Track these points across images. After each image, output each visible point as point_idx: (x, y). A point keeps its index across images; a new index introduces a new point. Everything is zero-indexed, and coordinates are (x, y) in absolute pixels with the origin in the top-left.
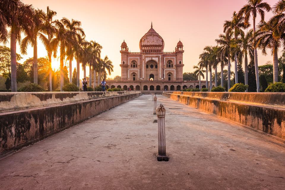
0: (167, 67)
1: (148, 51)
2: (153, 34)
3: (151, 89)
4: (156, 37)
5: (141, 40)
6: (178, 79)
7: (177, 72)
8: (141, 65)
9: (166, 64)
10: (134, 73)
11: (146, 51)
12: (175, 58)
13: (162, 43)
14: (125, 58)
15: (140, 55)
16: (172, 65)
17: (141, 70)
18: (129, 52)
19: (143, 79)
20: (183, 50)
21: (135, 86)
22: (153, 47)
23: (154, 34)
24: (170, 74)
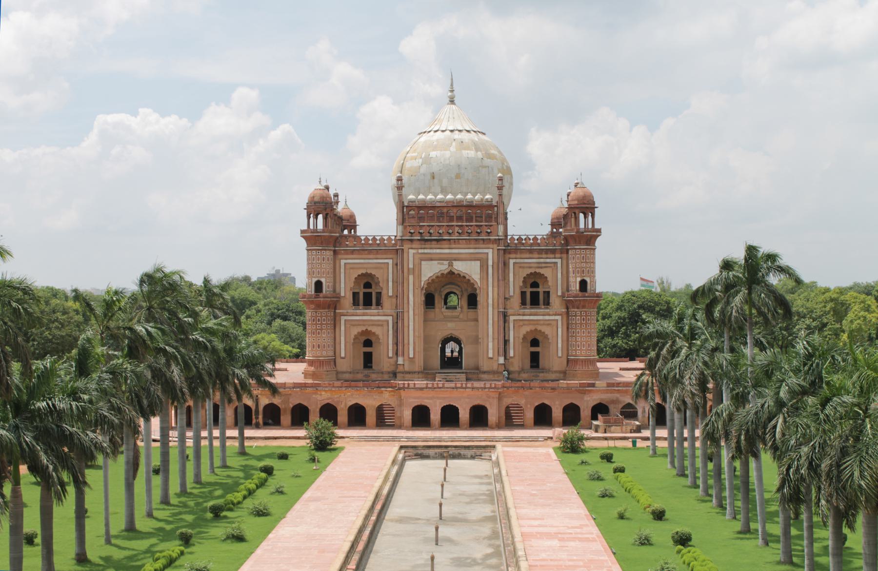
0: (523, 303)
2: (456, 135)
5: (399, 179)
6: (576, 361)
8: (399, 296)
9: (518, 292)
10: (366, 332)
12: (559, 261)
13: (500, 195)
14: (327, 266)
15: (393, 249)
16: (547, 294)
17: (399, 319)
19: (411, 360)
20: (596, 227)
21: (370, 402)
23: (465, 136)
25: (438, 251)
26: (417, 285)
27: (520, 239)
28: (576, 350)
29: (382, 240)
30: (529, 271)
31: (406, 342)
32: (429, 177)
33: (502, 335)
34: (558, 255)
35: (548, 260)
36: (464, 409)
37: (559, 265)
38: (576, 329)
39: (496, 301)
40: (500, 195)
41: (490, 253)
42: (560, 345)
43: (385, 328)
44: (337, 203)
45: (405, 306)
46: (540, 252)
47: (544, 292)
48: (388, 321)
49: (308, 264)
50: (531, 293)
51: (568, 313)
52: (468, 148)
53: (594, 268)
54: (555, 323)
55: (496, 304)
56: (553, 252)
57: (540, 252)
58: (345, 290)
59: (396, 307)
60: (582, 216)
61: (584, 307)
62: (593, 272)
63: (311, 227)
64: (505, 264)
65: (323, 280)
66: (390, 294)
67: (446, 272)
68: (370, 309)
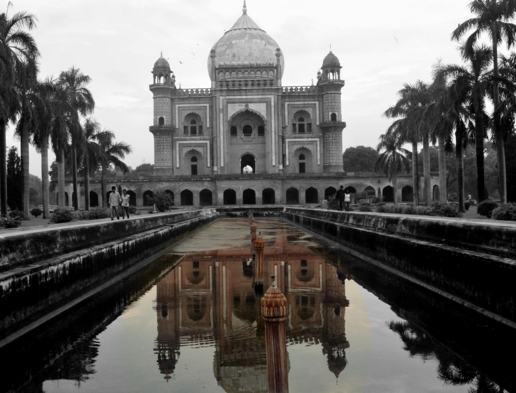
0: (294, 130)
1: (234, 85)
2: (248, 31)
3: (245, 202)
4: (259, 41)
5: (213, 51)
6: (330, 166)
7: (325, 145)
9: (291, 123)
10: (193, 152)
11: (227, 85)
12: (317, 103)
13: (278, 60)
14: (167, 108)
15: (208, 97)
16: (310, 125)
18: (178, 88)
19: (222, 169)
20: (341, 79)
21: (196, 188)
22: (249, 70)
23: (253, 31)
24: (303, 154)
25: (238, 97)
26: (225, 119)
27: (291, 89)
28: (329, 160)
29: (202, 91)
30: (297, 110)
31: (219, 156)
32: (231, 55)
33: (281, 151)
34: (316, 99)
35: (310, 102)
36: (259, 191)
37: (317, 105)
38: (329, 145)
39: (277, 128)
40: (278, 60)
41: (272, 98)
42: (319, 157)
43: (205, 148)
44: (174, 81)
45: (218, 133)
46: (305, 97)
47: (308, 124)
48: (206, 144)
49: (154, 107)
50: (299, 125)
51: (324, 137)
52: (256, 38)
53: (340, 106)
54: (315, 143)
55: (277, 131)
56: (313, 97)
57: (305, 97)
58: (179, 124)
59: (212, 134)
60: (331, 74)
61: (335, 131)
62: (340, 109)
63: (156, 82)
64: (282, 105)
65: (164, 117)
66: (208, 126)
67: (243, 111)
68: (195, 136)
